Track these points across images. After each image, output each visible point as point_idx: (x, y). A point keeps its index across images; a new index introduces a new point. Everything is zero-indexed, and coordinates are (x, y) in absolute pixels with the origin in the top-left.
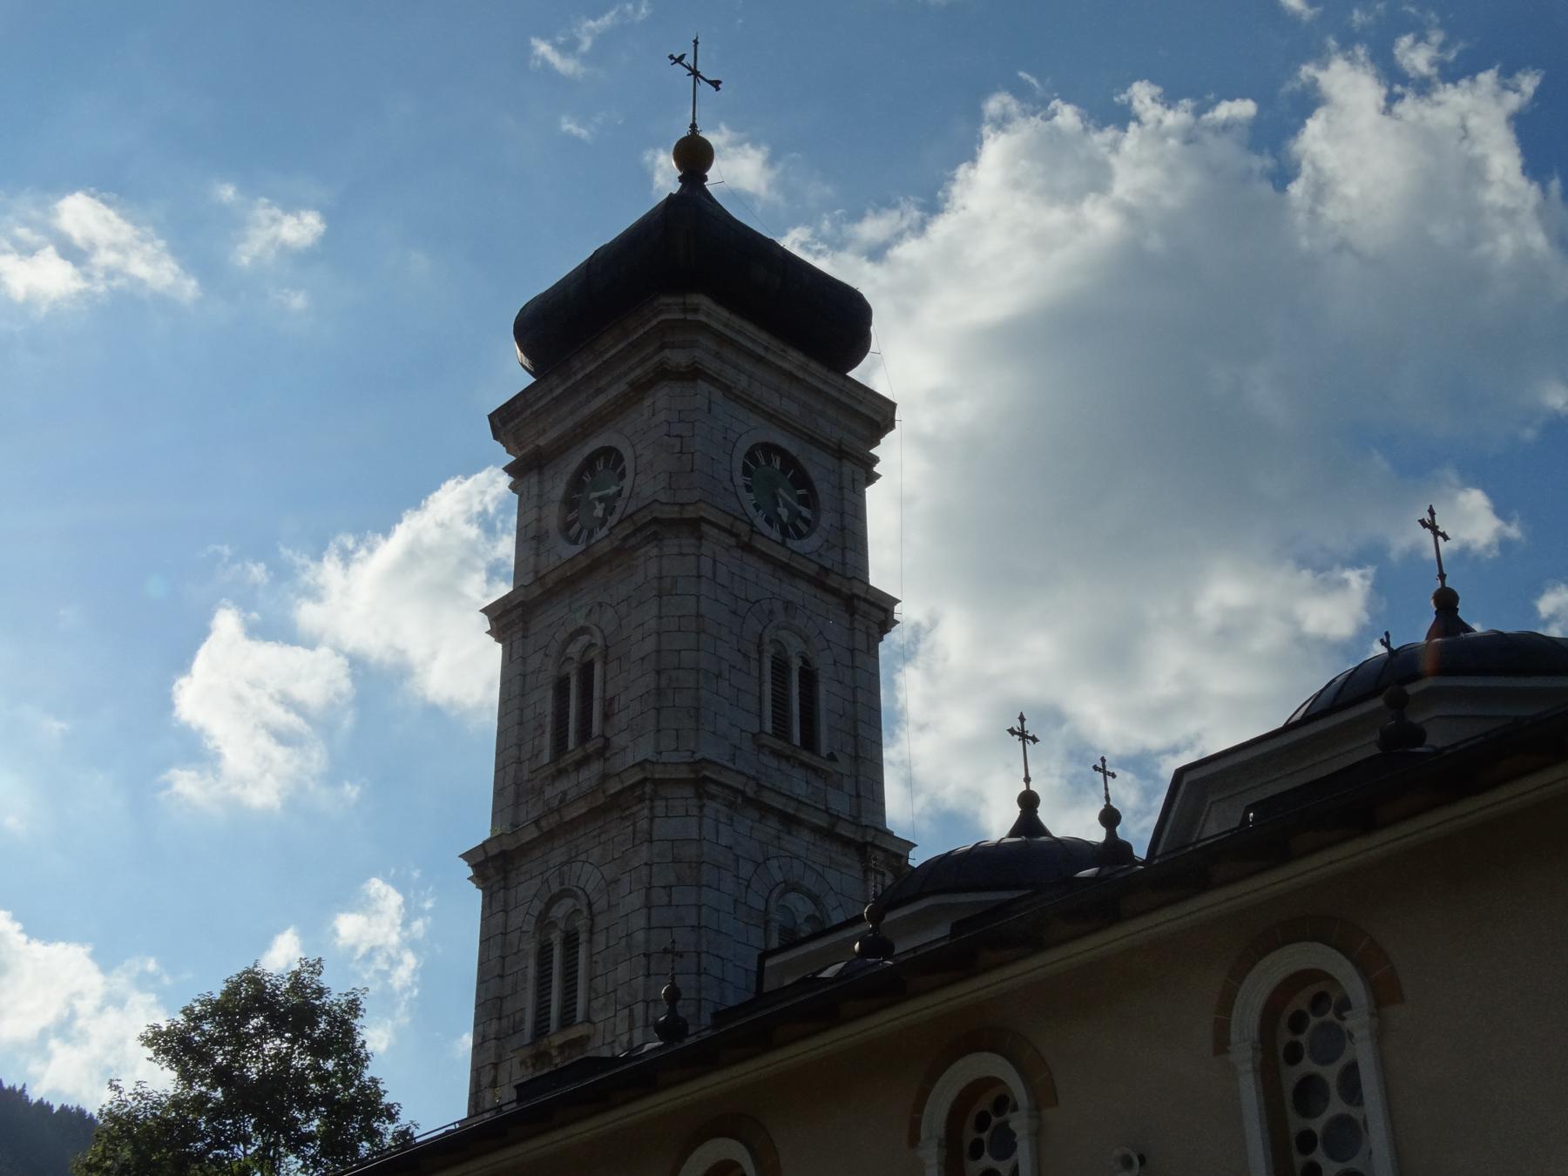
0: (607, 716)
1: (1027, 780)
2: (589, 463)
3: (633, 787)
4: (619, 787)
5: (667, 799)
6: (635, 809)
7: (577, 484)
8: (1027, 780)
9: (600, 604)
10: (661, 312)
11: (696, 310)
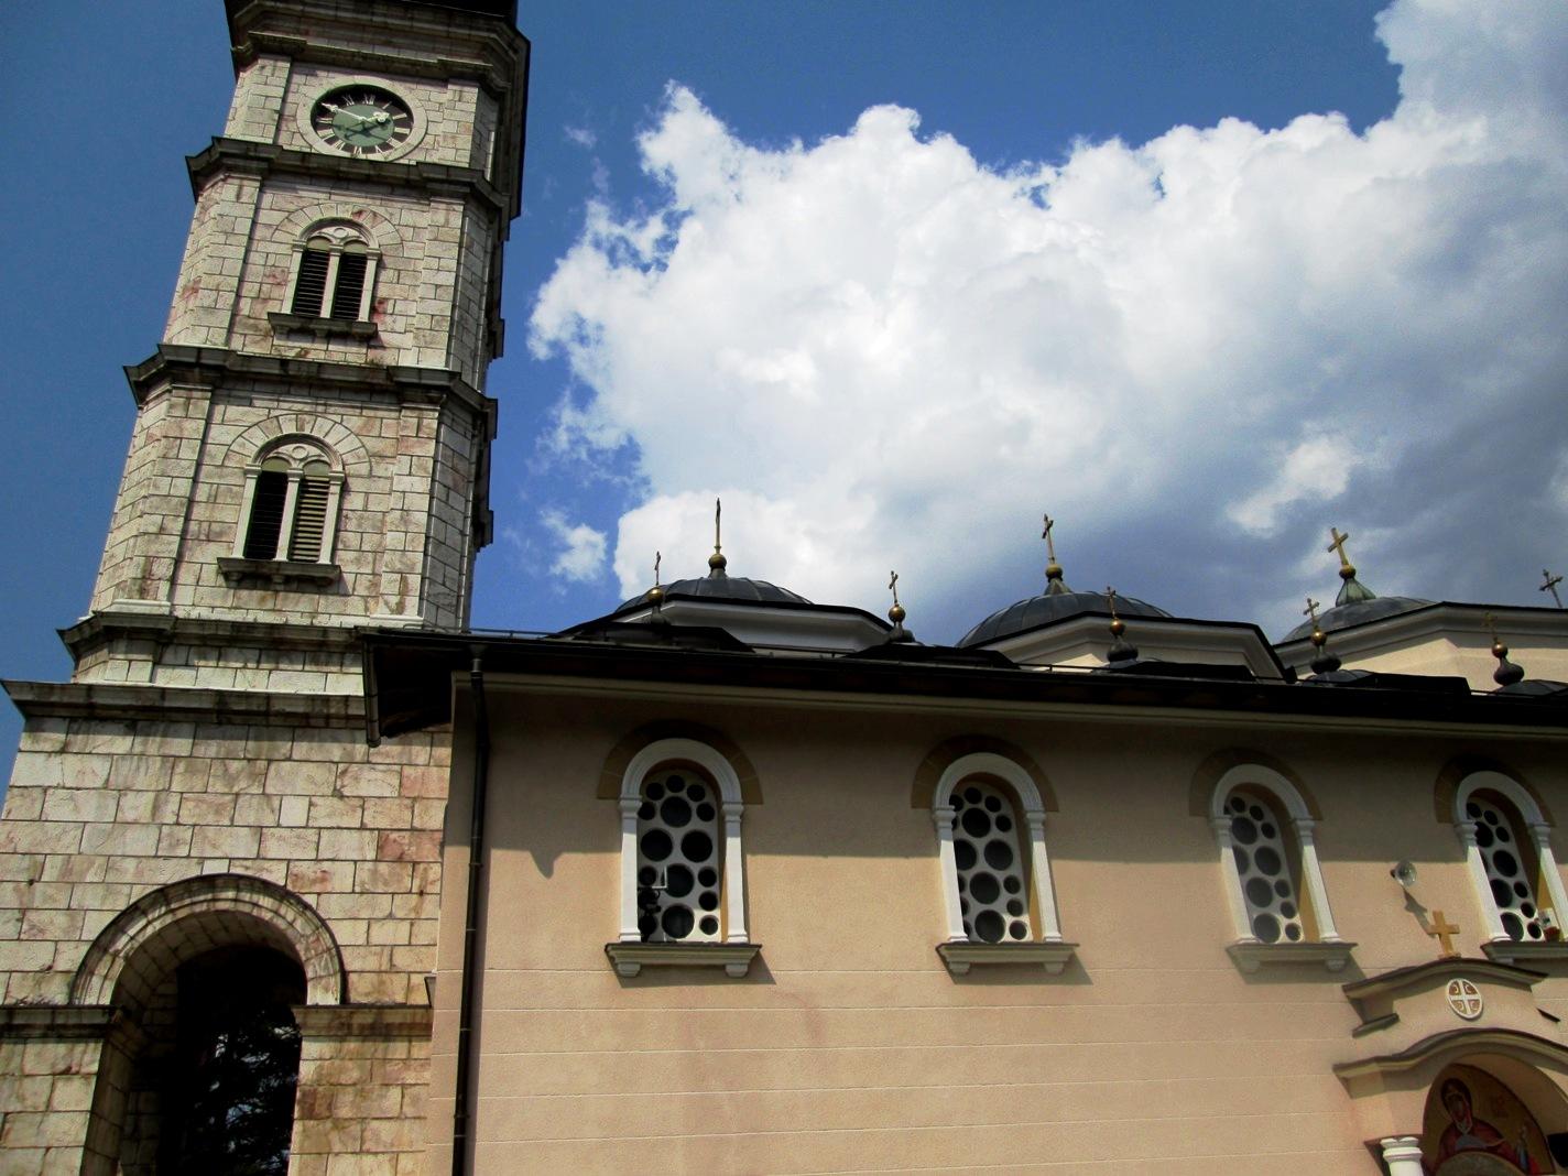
0: (373, 310)
1: (718, 548)
2: (358, 93)
3: (429, 388)
4: (415, 381)
5: (453, 414)
6: (423, 407)
7: (337, 96)
8: (718, 548)
9: (375, 214)
10: (495, 31)
11: (516, 51)
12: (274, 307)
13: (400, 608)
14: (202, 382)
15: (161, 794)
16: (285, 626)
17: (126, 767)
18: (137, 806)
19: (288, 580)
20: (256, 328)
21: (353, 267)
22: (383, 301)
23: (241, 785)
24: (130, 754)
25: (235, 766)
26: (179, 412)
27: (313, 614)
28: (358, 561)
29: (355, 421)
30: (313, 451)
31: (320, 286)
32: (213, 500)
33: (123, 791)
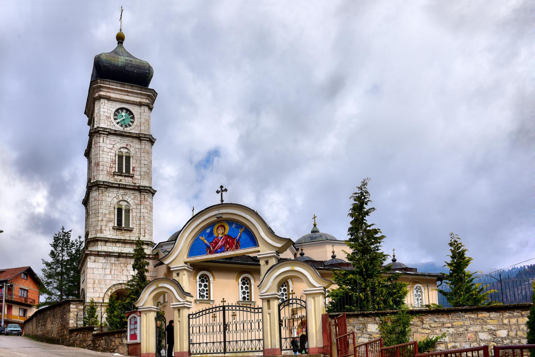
12: (113, 170)
13: (144, 236)
14: (104, 188)
15: (111, 270)
16: (126, 240)
17: (105, 265)
18: (108, 271)
19: (125, 230)
20: (111, 174)
21: (128, 158)
22: (134, 168)
23: (123, 268)
24: (105, 263)
25: (122, 265)
26: (101, 195)
27: (130, 237)
28: (136, 226)
29: (132, 197)
30: (126, 203)
31: (122, 164)
32: (109, 213)
33: (105, 269)
